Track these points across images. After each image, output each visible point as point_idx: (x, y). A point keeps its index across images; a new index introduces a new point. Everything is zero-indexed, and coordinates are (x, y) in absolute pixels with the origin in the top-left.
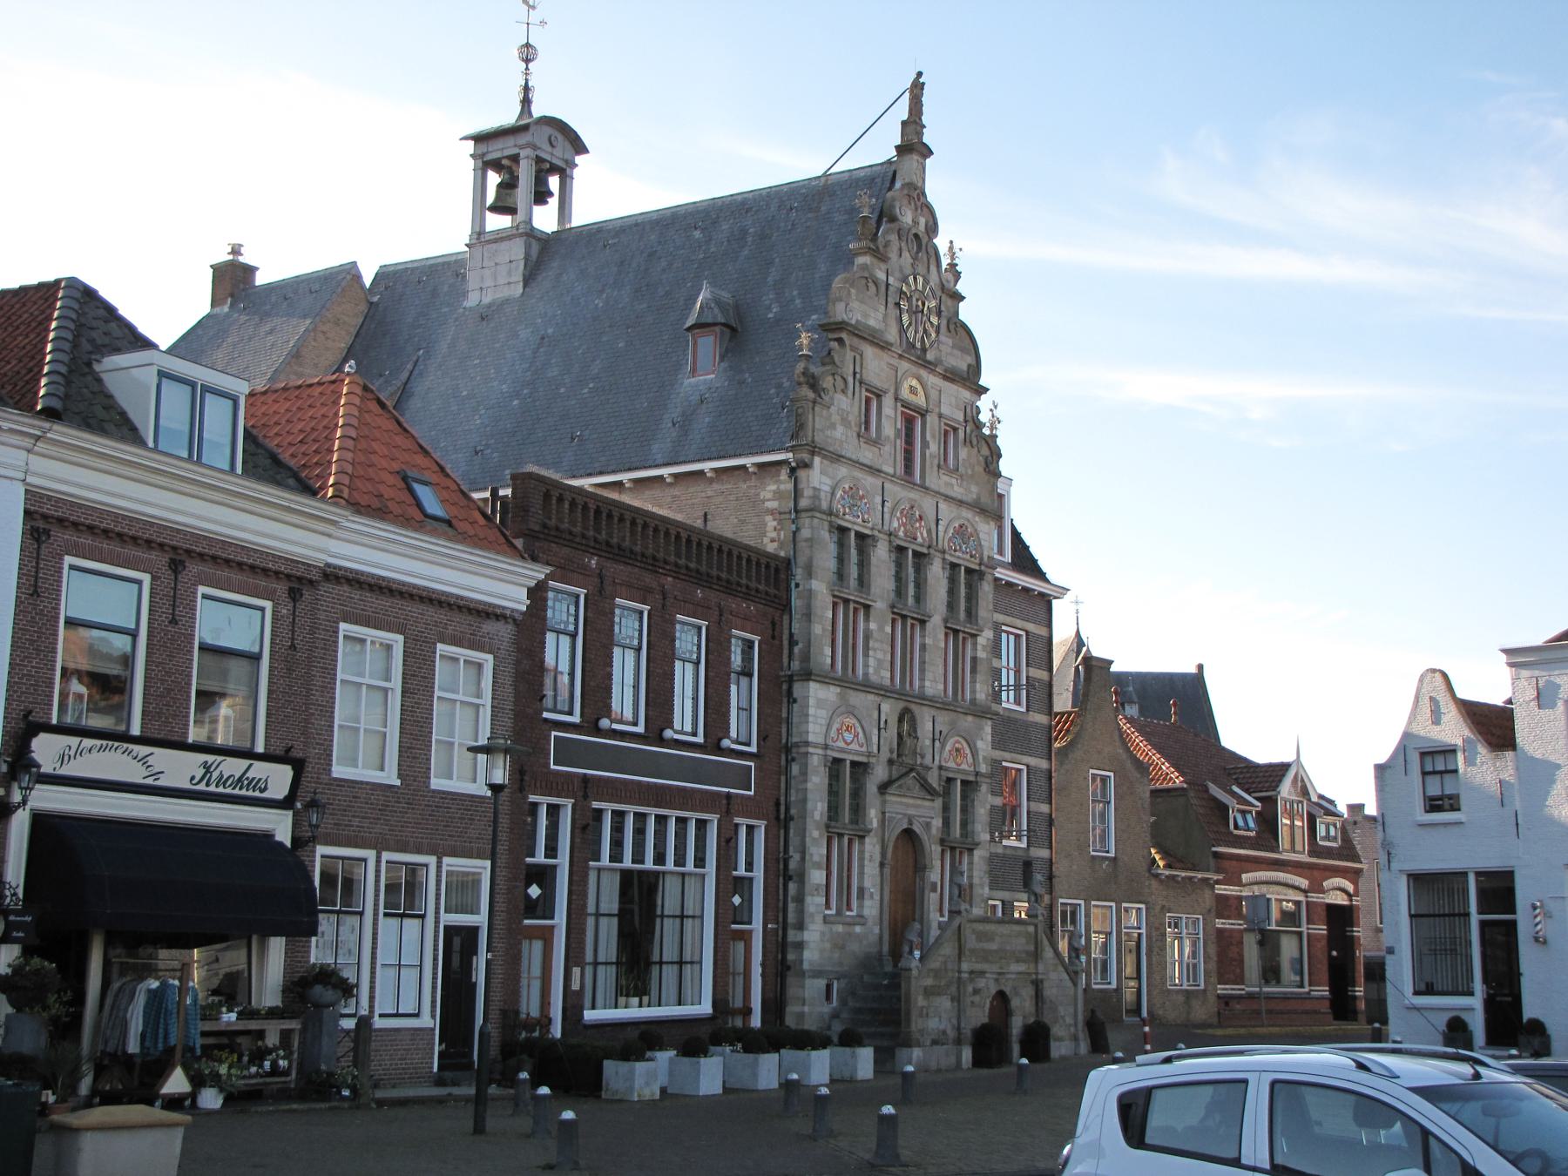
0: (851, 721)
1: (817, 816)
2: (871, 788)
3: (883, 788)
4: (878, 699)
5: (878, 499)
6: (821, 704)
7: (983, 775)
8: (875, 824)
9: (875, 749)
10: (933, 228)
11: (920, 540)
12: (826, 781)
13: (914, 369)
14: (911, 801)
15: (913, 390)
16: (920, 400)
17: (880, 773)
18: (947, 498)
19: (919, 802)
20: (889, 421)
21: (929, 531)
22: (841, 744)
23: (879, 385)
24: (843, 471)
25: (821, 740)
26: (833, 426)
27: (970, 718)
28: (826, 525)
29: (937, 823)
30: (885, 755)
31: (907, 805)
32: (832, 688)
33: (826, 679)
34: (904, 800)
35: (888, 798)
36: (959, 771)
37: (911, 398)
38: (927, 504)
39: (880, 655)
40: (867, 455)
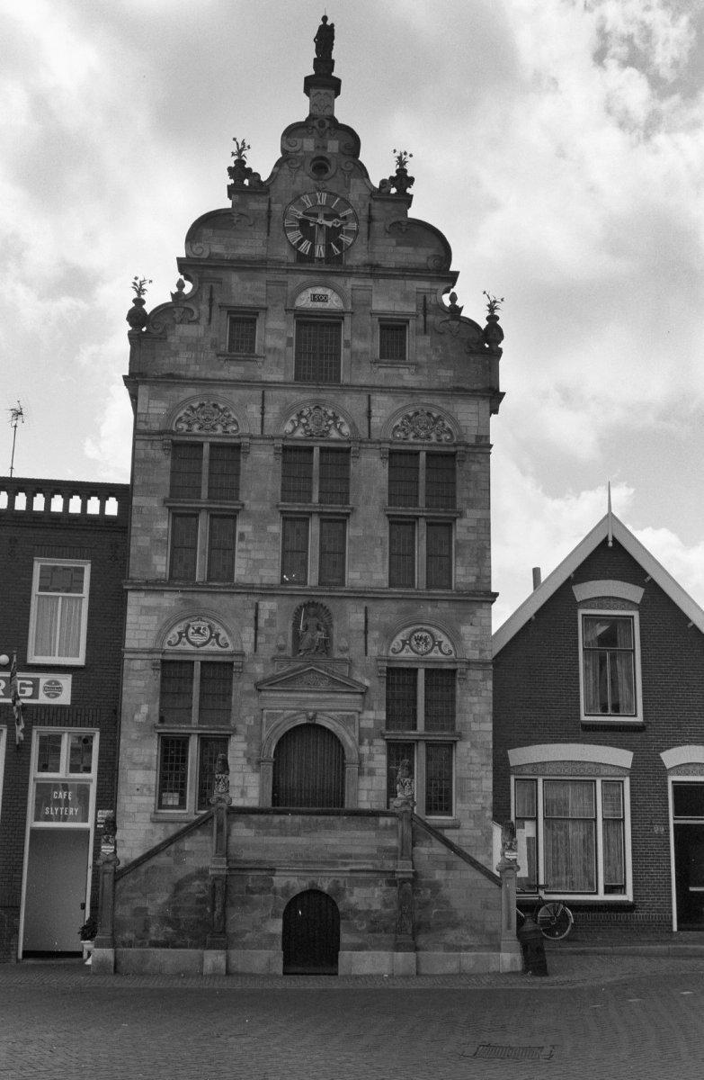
0: (203, 625)
1: (139, 717)
2: (241, 686)
3: (259, 688)
4: (255, 599)
5: (254, 410)
6: (147, 610)
7: (469, 663)
8: (250, 720)
9: (248, 648)
10: (352, 141)
11: (334, 434)
12: (157, 684)
13: (315, 278)
14: (311, 696)
15: (315, 298)
16: (334, 303)
17: (259, 670)
18: (383, 389)
19: (327, 696)
20: (275, 333)
21: (353, 426)
22: (189, 647)
23: (250, 303)
24: (191, 391)
25: (148, 645)
26: (176, 354)
27: (446, 605)
28: (158, 445)
29: (374, 716)
30: (267, 650)
31: (307, 700)
32: (166, 595)
33: (153, 586)
34: (293, 695)
35: (263, 694)
36: (417, 661)
37: (319, 305)
38: (352, 404)
39: (260, 556)
40: (235, 371)
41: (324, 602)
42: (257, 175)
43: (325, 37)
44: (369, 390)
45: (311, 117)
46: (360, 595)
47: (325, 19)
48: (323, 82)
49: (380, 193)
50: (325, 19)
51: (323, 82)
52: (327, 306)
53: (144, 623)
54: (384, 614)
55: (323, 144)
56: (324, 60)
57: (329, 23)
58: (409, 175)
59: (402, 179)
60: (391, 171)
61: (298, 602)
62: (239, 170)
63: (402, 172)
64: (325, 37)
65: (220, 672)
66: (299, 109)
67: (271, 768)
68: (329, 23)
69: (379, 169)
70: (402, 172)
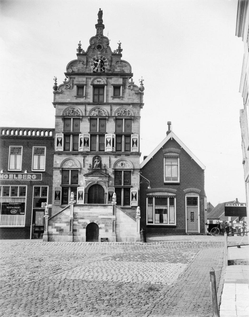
41: (99, 155)
42: (84, 51)
43: (100, 14)
44: (111, 104)
45: (97, 35)
46: (108, 154)
47: (100, 9)
48: (100, 26)
49: (114, 55)
50: (100, 9)
51: (100, 26)
52: (101, 83)
53: (58, 161)
54: (114, 159)
55: (99, 42)
56: (100, 20)
57: (101, 10)
58: (121, 48)
59: (120, 50)
60: (117, 48)
61: (94, 156)
62: (80, 50)
63: (119, 47)
64: (100, 14)
65: (76, 173)
66: (94, 33)
67: (87, 195)
68: (101, 10)
69: (113, 47)
70: (119, 47)
